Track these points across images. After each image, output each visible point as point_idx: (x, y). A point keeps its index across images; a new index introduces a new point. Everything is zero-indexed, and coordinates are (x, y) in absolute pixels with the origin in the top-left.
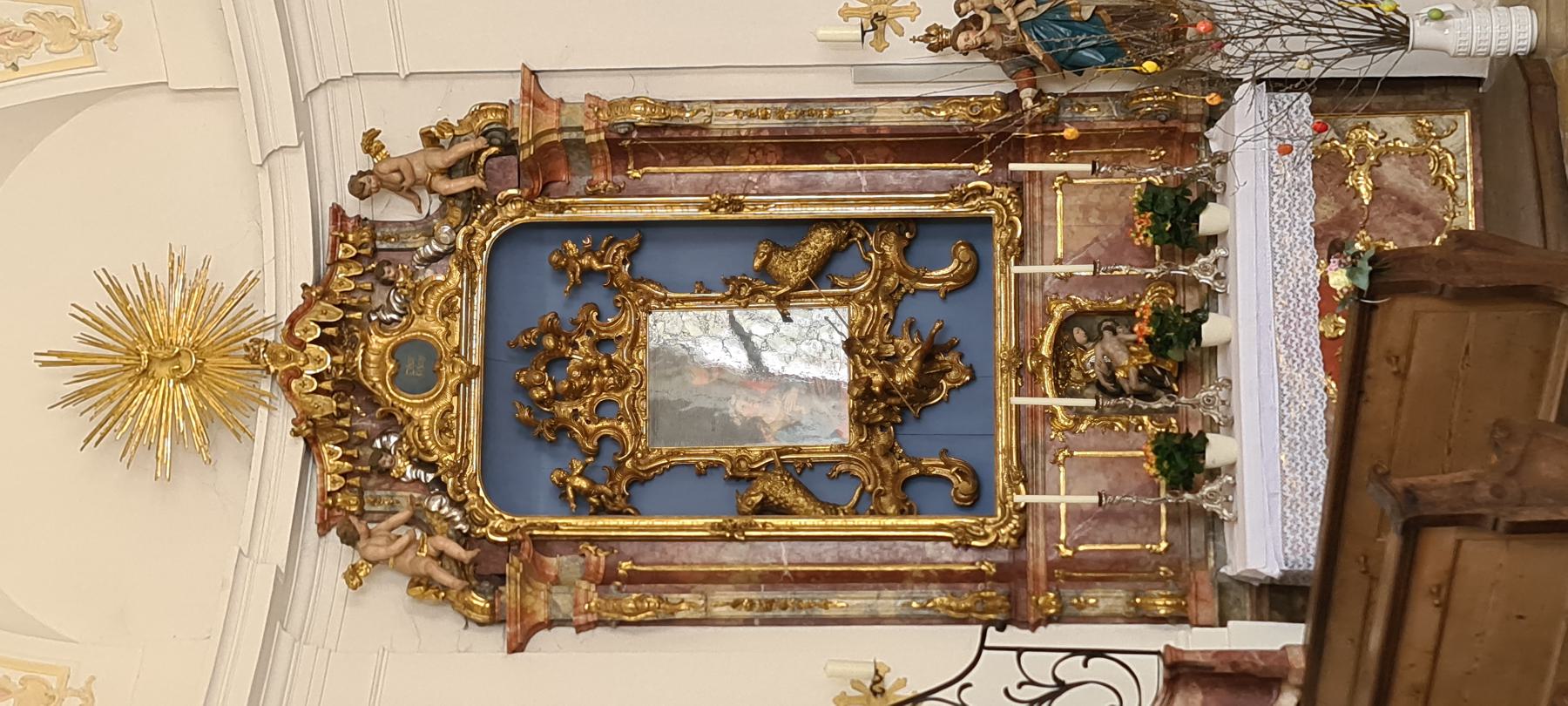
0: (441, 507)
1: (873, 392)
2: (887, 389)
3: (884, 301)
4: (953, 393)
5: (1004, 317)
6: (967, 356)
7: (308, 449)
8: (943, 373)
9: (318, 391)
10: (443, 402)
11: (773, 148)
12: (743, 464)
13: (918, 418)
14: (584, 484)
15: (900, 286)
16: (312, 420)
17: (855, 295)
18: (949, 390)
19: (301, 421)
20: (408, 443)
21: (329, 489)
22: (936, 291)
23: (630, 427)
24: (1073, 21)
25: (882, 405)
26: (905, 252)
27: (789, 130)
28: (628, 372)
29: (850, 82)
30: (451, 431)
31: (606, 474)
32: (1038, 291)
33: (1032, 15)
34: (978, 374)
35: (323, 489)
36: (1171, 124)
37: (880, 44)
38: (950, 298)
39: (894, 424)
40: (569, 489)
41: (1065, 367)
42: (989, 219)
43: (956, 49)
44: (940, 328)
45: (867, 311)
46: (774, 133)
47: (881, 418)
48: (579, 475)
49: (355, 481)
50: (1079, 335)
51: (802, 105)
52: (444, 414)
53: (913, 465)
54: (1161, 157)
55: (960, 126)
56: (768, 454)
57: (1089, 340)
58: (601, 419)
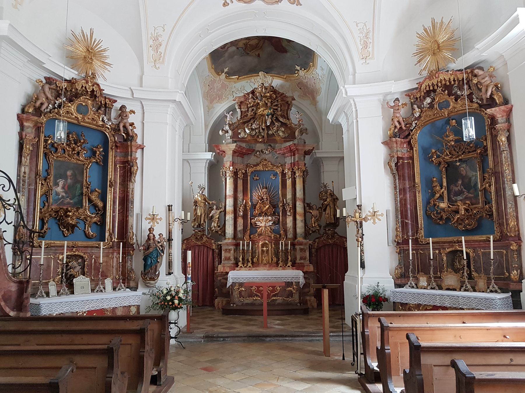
0: (50, 107)
1: (67, 212)
2: (68, 216)
3: (85, 217)
4: (61, 232)
5: (85, 244)
6: (70, 235)
7: (66, 80)
8: (68, 231)
9: (82, 86)
10: (74, 114)
11: (123, 195)
12: (49, 181)
13: (57, 223)
14: (49, 142)
15: (87, 221)
16: (75, 83)
17: (86, 211)
18: (63, 231)
19: (76, 80)
20: (67, 103)
21: (57, 82)
22: (85, 229)
23: (59, 156)
24: (157, 257)
25: (62, 215)
26: (95, 223)
27: (129, 199)
28: (72, 157)
29: (137, 213)
30: (67, 114)
31: (50, 148)
32: (90, 251)
33: (158, 249)
34: (65, 238)
35: (57, 81)
36: (126, 279)
37: (147, 219)
38: (83, 232)
39: (56, 218)
40: (48, 138)
41: (71, 257)
42: (105, 241)
43: (149, 234)
44: (80, 229)
45: (83, 213)
46: (127, 196)
47: (60, 214)
48: (51, 142)
49: (58, 89)
50: (80, 261)
51: (132, 203)
52: (71, 113)
53: (47, 221)
54: (116, 279)
55: (128, 235)
56: (51, 187)
57: (78, 263)
58: (61, 149)
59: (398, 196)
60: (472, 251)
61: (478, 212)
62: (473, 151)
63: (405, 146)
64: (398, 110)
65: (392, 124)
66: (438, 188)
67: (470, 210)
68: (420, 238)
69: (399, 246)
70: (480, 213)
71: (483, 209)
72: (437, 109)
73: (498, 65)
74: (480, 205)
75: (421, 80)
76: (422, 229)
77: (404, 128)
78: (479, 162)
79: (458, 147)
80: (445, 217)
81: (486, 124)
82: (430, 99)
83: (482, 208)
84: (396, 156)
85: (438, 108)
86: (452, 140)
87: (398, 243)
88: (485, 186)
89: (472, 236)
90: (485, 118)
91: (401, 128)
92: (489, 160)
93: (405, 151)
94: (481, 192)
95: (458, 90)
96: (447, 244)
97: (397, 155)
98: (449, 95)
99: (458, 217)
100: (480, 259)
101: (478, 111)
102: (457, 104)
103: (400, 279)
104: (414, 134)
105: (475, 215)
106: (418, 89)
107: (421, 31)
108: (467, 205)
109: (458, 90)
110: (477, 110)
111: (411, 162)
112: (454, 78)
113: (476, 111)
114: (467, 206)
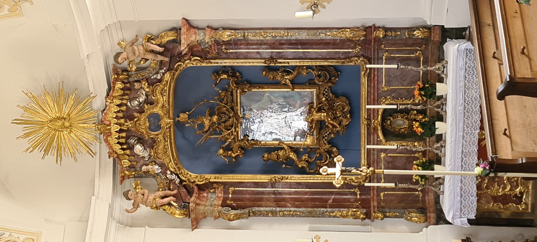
59: (288, 209)
60: (384, 99)
61: (324, 94)
62: (232, 95)
63: (205, 195)
64: (143, 195)
65: (164, 210)
66: (281, 153)
67: (321, 105)
68: (360, 182)
69: (372, 212)
70: (326, 92)
71: (320, 86)
72: (157, 135)
73: (117, 37)
74: (314, 91)
75: (106, 150)
76: (346, 178)
77: (175, 192)
78: (249, 87)
79: (222, 115)
80: (327, 146)
81: (199, 65)
82: (138, 145)
83: (319, 88)
84: (220, 208)
85: (156, 133)
86: (210, 120)
87: (368, 216)
88: (287, 80)
89: (361, 99)
90: (189, 65)
91: (174, 196)
92: (251, 64)
93: (214, 196)
94: (295, 88)
95: (138, 99)
96: (372, 136)
97: (218, 206)
98: (141, 111)
99: (329, 120)
100: (396, 89)
101: (177, 73)
102: (158, 103)
103: (428, 215)
104: (189, 179)
105: (329, 99)
106: (117, 159)
107: (26, 143)
108: (313, 110)
109: (138, 99)
110: (174, 74)
111: (231, 189)
112: (119, 99)
113: (175, 77)
114: (313, 110)
